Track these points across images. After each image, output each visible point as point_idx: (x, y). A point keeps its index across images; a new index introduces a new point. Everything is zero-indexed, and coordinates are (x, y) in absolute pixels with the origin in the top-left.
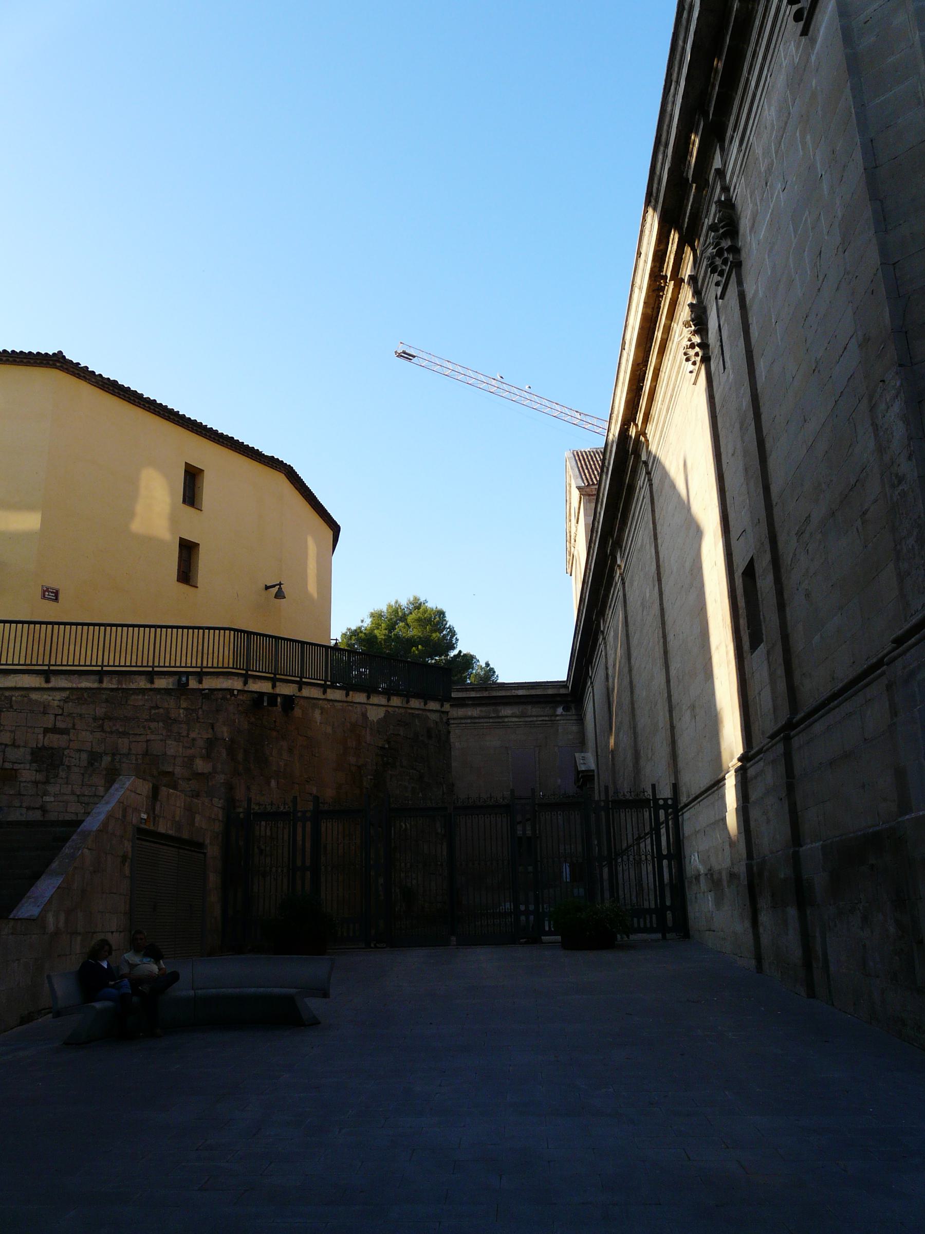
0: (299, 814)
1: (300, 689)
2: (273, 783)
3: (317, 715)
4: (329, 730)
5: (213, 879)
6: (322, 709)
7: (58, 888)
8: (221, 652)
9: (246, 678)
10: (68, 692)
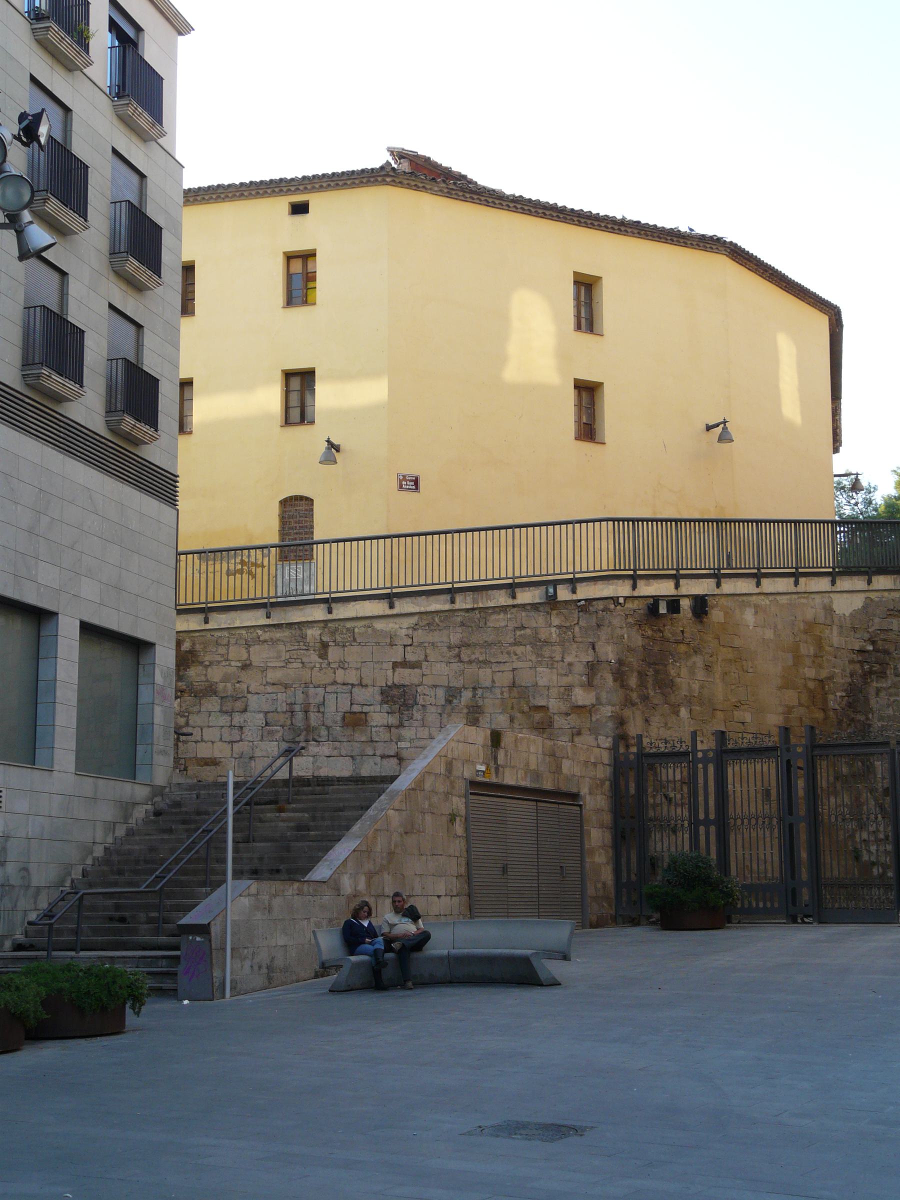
0: (700, 755)
1: (718, 585)
2: (684, 712)
3: (749, 616)
4: (769, 634)
5: (598, 837)
6: (756, 607)
7: (354, 851)
8: (598, 552)
9: (634, 579)
10: (416, 618)
